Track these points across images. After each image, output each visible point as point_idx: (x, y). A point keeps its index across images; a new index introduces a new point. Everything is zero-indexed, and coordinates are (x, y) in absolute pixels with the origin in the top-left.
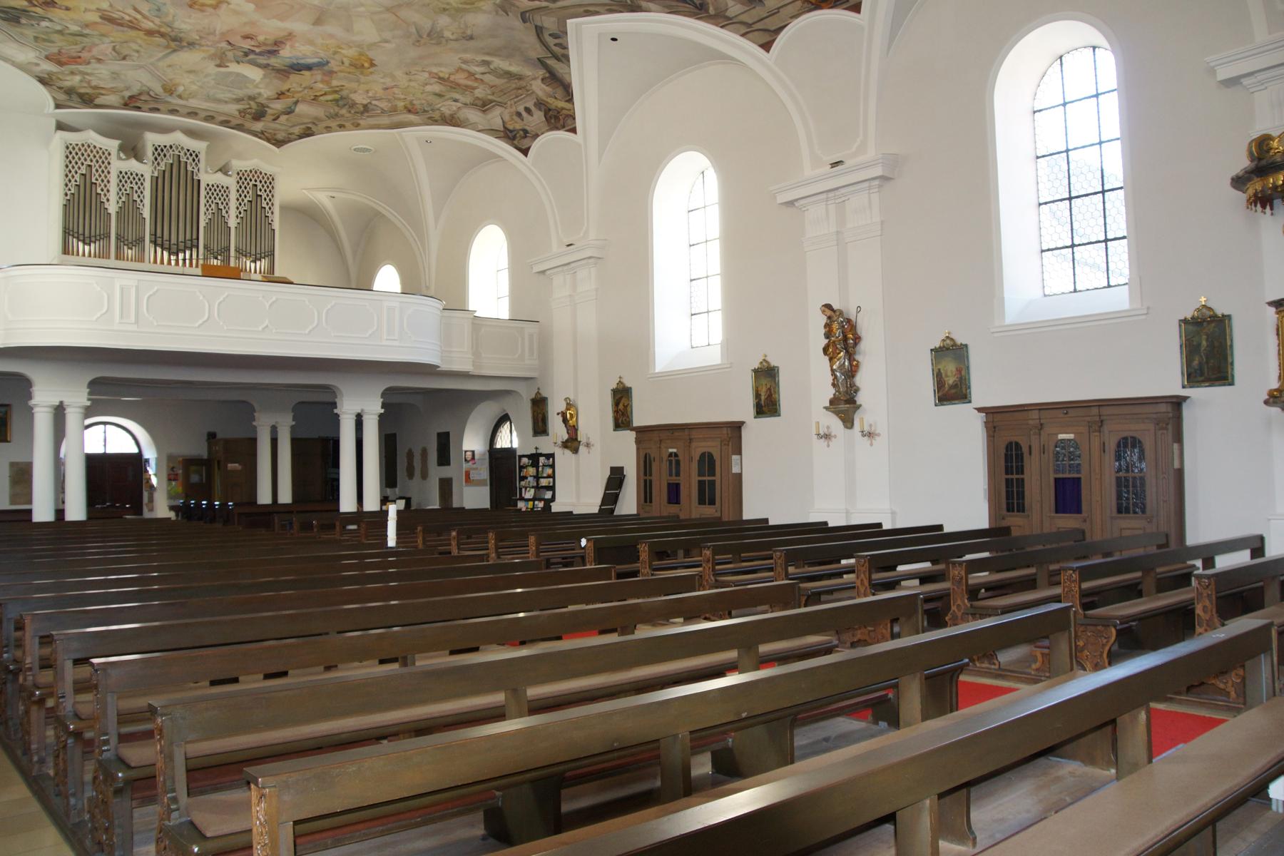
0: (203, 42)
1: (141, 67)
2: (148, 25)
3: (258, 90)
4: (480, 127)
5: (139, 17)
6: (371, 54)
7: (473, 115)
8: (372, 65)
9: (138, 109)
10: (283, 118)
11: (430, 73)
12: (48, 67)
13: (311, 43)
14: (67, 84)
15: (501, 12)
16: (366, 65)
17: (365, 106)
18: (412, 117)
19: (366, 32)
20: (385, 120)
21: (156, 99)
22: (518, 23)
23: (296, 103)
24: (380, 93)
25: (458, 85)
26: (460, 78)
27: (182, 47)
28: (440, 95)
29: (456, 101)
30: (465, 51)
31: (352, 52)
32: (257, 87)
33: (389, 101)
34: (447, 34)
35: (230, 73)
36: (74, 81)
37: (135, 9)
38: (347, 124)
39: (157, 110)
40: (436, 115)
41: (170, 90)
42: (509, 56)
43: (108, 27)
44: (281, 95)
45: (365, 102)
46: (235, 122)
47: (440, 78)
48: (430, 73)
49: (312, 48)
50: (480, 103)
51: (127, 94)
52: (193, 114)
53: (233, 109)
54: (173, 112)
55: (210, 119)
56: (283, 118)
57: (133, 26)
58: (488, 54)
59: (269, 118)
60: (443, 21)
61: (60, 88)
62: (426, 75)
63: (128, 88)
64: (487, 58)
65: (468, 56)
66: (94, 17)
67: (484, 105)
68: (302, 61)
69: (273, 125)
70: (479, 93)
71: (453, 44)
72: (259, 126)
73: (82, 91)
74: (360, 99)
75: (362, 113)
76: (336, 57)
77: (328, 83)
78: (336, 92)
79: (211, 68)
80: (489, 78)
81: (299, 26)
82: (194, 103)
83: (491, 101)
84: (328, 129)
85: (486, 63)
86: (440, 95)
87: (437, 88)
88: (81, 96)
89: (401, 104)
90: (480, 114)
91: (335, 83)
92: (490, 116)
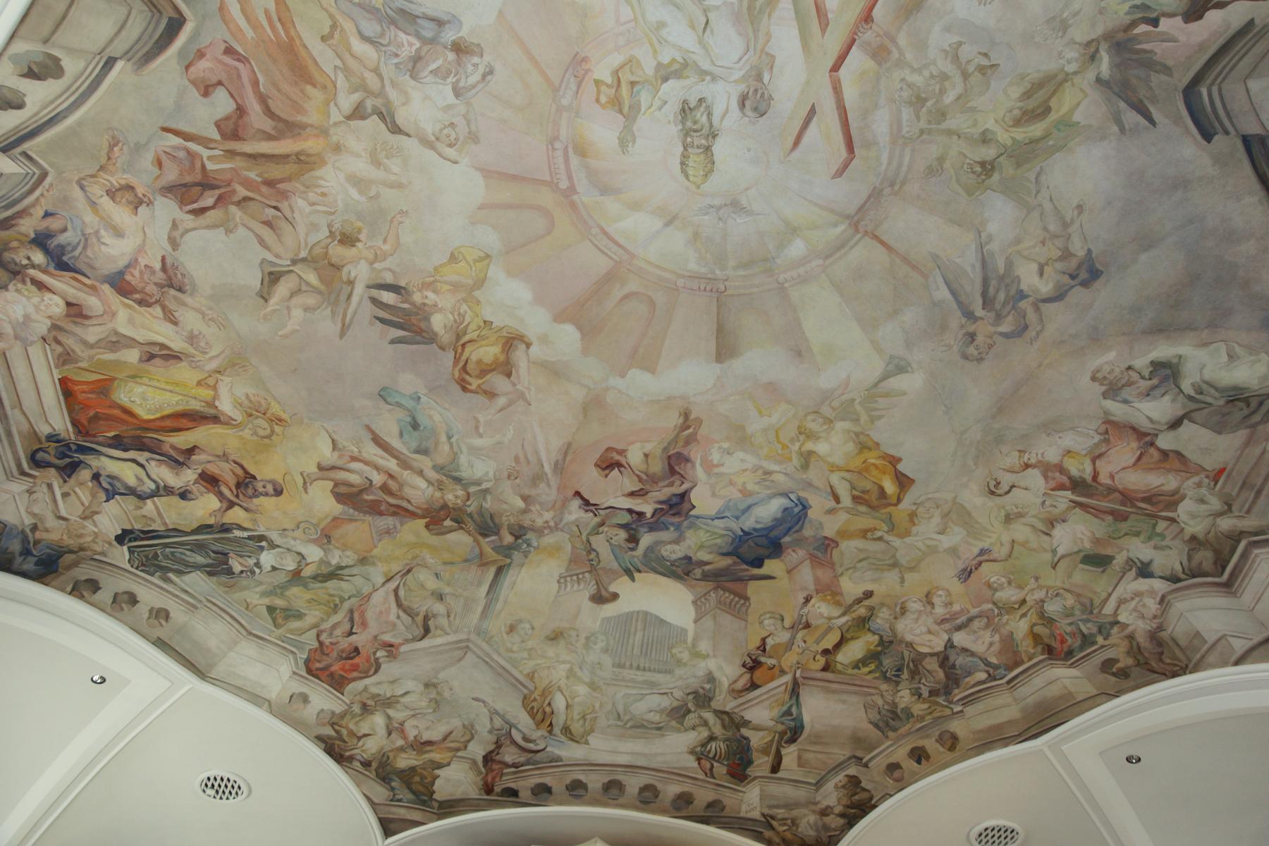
0: (540, 517)
1: (465, 647)
2: (419, 490)
3: (702, 667)
4: (1239, 646)
5: (392, 464)
6: (886, 435)
7: (1202, 613)
8: (904, 482)
9: (511, 796)
10: (790, 754)
11: (1047, 469)
12: (322, 700)
13: (742, 439)
14: (371, 747)
15: (1131, 117)
16: (890, 487)
17: (943, 659)
18: (1062, 678)
19: (844, 346)
20: (1003, 707)
21: (532, 754)
22: (1189, 150)
23: (795, 691)
24: (958, 596)
25: (1127, 497)
26: (1122, 467)
27: (506, 551)
28: (1098, 561)
29: (1144, 571)
30: (1096, 338)
31: (834, 446)
32: (696, 655)
33: (990, 621)
34: (1029, 277)
35: (629, 617)
36: (374, 736)
37: (378, 441)
38: (930, 744)
39: (542, 793)
40: (1117, 649)
41: (543, 717)
42: (1215, 324)
43: (361, 529)
44: (754, 667)
45: (938, 644)
46: (704, 795)
47: (1077, 485)
48: (1047, 469)
49: (751, 460)
50: (1205, 557)
51: (477, 750)
52: (612, 791)
53: (675, 748)
54: (576, 791)
55: (648, 798)
56: (790, 754)
57: (403, 512)
58: (1160, 330)
59: (761, 764)
60: (1000, 216)
61: (366, 764)
62: (1035, 479)
63: (470, 731)
64: (1163, 351)
65: (1108, 359)
66: (322, 502)
67: (1221, 564)
68: (749, 523)
69: (776, 789)
70: (1195, 514)
71: (1059, 318)
72: (750, 800)
73: (404, 761)
74: (922, 633)
75: (947, 692)
76: (813, 475)
77: (830, 591)
78: (863, 623)
79: (592, 617)
80: (1194, 440)
81: (689, 376)
82: (606, 748)
83: (1235, 537)
84: (897, 776)
85: (1166, 373)
86: (1098, 561)
87: (1077, 532)
88: (407, 776)
89: (1020, 627)
90: (1219, 600)
91: (851, 587)
92: (1247, 597)
